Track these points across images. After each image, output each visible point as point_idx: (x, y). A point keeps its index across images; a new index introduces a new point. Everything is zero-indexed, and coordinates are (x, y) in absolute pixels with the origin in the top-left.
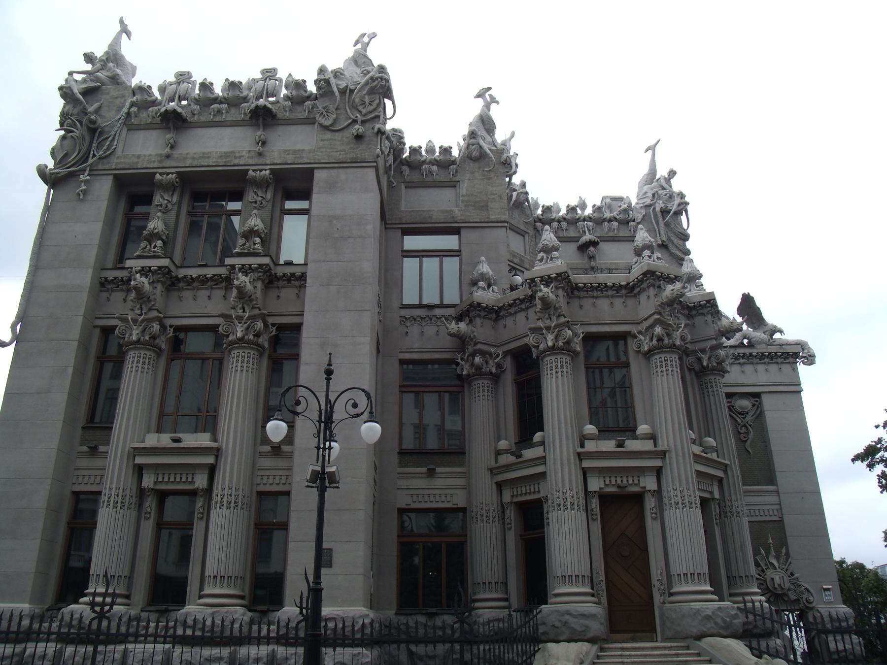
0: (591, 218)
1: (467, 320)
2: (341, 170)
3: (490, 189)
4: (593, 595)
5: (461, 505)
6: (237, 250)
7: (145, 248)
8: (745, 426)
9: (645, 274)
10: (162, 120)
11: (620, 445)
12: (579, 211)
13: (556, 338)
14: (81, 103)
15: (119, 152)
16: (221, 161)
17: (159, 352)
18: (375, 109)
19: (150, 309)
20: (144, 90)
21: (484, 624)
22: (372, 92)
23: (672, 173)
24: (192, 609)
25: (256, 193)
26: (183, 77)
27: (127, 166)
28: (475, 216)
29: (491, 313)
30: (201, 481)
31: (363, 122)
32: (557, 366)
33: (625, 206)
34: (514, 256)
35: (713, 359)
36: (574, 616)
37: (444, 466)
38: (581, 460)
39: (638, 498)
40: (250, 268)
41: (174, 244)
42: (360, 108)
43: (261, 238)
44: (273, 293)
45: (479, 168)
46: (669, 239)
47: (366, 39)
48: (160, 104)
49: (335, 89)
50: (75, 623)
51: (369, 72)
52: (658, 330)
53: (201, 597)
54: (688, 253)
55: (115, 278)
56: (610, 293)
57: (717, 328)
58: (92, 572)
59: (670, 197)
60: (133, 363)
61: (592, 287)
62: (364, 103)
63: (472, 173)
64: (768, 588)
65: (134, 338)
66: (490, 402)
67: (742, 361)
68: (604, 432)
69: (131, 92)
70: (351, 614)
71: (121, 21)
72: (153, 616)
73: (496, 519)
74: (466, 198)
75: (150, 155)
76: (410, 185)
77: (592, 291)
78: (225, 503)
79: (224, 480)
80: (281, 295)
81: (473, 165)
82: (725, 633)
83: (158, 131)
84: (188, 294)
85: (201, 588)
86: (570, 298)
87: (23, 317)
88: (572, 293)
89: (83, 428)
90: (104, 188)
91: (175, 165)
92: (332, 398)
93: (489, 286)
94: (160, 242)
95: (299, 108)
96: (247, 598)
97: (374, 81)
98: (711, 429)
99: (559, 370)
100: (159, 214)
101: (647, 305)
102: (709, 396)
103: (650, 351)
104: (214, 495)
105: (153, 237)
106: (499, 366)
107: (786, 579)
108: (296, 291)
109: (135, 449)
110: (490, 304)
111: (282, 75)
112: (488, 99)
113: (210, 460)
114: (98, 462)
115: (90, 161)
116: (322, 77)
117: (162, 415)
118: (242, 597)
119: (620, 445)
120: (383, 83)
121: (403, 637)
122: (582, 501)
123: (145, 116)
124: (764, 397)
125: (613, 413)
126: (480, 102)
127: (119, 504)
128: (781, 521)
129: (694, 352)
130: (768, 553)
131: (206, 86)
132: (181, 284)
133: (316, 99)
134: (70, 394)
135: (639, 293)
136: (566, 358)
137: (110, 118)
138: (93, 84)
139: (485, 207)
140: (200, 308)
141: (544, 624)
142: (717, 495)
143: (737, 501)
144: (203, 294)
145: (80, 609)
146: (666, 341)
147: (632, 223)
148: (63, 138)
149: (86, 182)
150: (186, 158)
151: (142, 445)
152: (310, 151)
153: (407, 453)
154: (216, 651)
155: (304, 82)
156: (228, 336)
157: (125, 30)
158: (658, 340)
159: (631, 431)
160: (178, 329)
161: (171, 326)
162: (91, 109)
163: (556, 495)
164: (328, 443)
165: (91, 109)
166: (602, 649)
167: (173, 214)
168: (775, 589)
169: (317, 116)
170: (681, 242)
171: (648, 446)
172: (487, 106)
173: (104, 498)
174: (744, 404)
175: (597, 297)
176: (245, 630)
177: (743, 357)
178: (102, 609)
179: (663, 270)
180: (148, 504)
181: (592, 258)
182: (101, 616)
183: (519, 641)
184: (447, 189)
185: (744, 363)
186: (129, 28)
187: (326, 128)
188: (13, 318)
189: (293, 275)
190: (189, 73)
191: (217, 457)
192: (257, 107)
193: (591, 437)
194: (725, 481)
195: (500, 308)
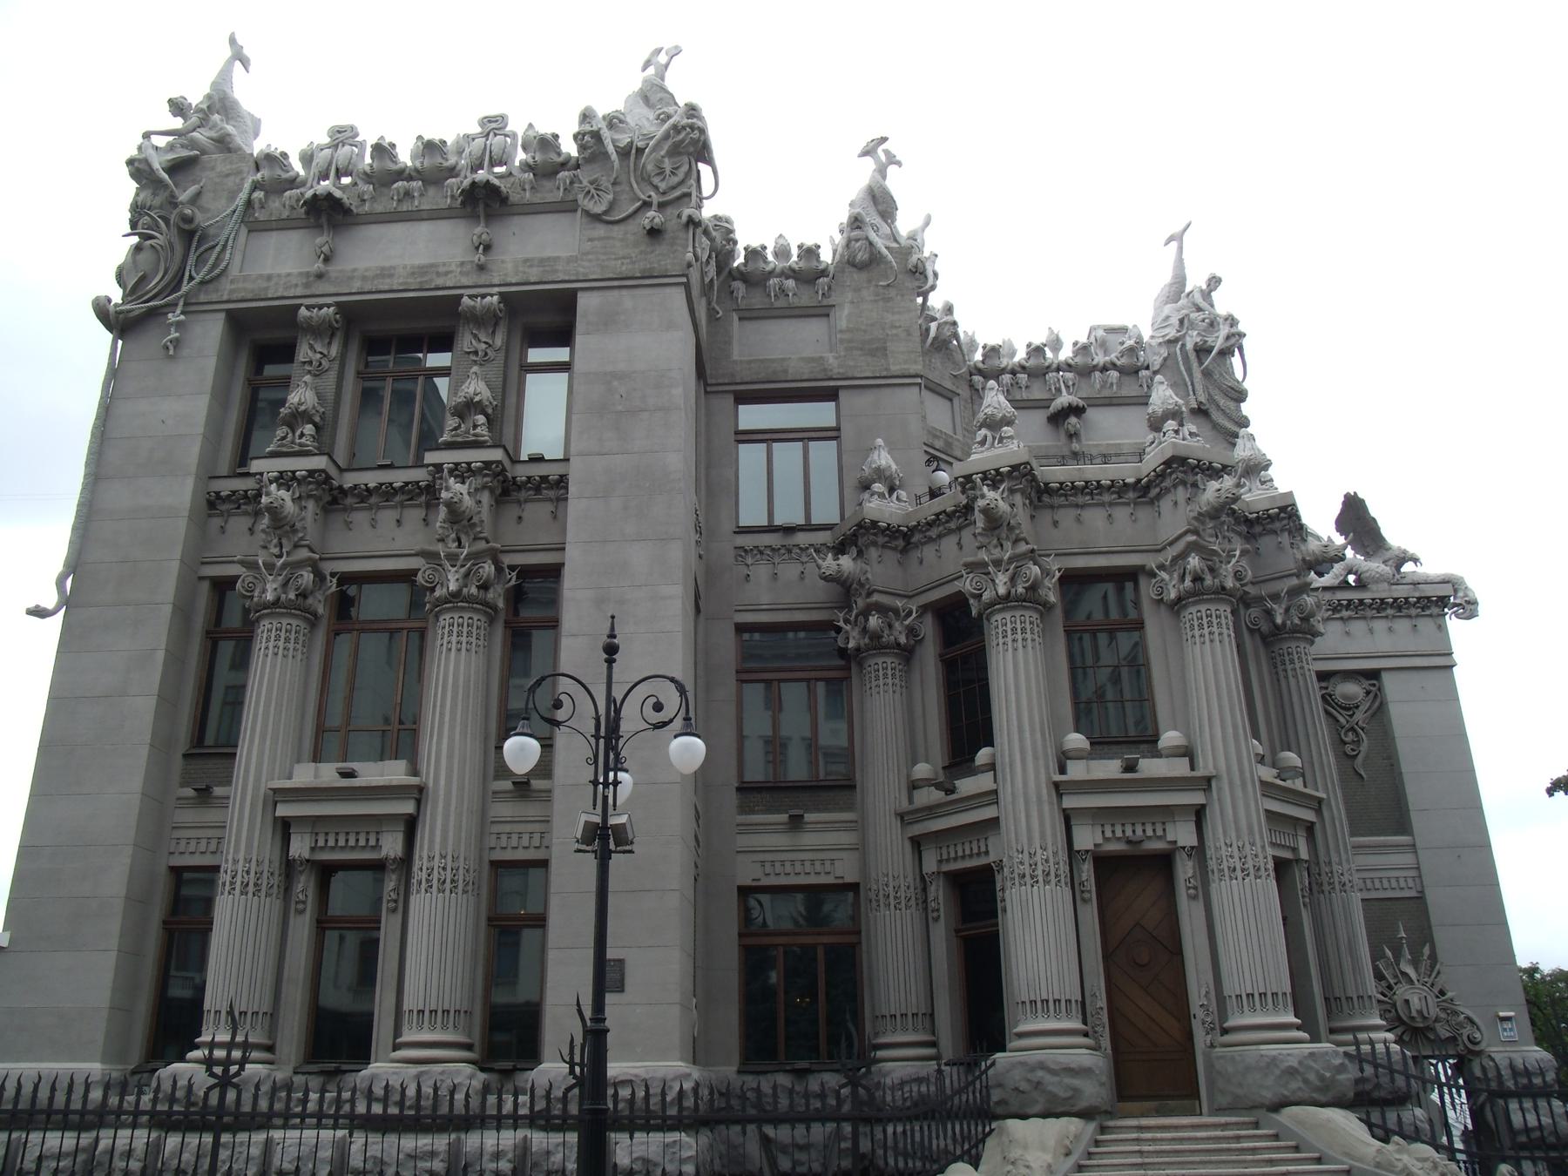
0: (1069, 365)
1: (854, 551)
2: (624, 292)
3: (889, 317)
4: (1086, 1035)
5: (849, 879)
6: (445, 437)
7: (283, 438)
8: (1352, 729)
9: (1168, 463)
10: (307, 213)
11: (1130, 767)
12: (1049, 354)
13: (1013, 579)
14: (166, 186)
15: (234, 271)
16: (413, 282)
17: (313, 620)
19: (296, 546)
20: (274, 160)
21: (893, 1088)
22: (675, 151)
23: (1214, 282)
24: (382, 1069)
25: (475, 336)
26: (343, 136)
27: (250, 296)
28: (863, 366)
30: (392, 845)
31: (662, 206)
32: (1014, 630)
33: (1132, 342)
34: (935, 436)
35: (1292, 611)
37: (819, 810)
38: (1060, 796)
39: (1164, 862)
40: (469, 469)
42: (656, 181)
43: (487, 415)
44: (511, 512)
45: (869, 281)
46: (1211, 399)
47: (663, 58)
48: (303, 184)
49: (611, 149)
50: (180, 1094)
51: (669, 117)
52: (1194, 562)
53: (396, 1047)
54: (1244, 423)
55: (234, 492)
56: (1106, 498)
57: (1299, 557)
58: (206, 1006)
59: (1212, 324)
60: (268, 640)
61: (1073, 487)
62: (661, 172)
63: (857, 290)
64: (1399, 1018)
65: (270, 596)
66: (897, 695)
67: (1345, 614)
68: (1101, 745)
69: (253, 165)
70: (660, 1074)
71: (232, 41)
72: (315, 1082)
73: (913, 902)
74: (846, 336)
75: (289, 275)
76: (748, 316)
77: (1075, 495)
78: (435, 882)
79: (431, 842)
80: (525, 515)
81: (859, 277)
82: (1323, 1099)
83: (302, 231)
84: (360, 518)
85: (397, 1032)
86: (1035, 508)
87: (75, 565)
88: (1039, 500)
89: (185, 756)
90: (210, 334)
91: (332, 290)
92: (618, 694)
93: (892, 490)
94: (310, 426)
95: (548, 184)
96: (477, 1047)
97: (679, 132)
98: (1292, 737)
99: (1019, 637)
100: (307, 378)
101: (1174, 517)
102: (1286, 677)
103: (1179, 599)
104: (415, 869)
105: (297, 418)
106: (911, 631)
107: (1432, 1001)
108: (549, 507)
109: (275, 791)
110: (894, 522)
111: (517, 126)
112: (883, 158)
113: (408, 808)
114: (211, 816)
115: (185, 288)
116: (587, 128)
117: (321, 730)
119: (1130, 767)
120: (696, 135)
121: (753, 1112)
122: (1064, 869)
123: (277, 207)
124: (1385, 677)
126: (869, 164)
127: (251, 888)
128: (1420, 899)
129: (1260, 600)
130: (1398, 955)
131: (383, 151)
132: (349, 501)
133: (578, 166)
134: (161, 697)
135: (1159, 497)
136: (1031, 616)
137: (218, 212)
138: (185, 153)
139: (878, 350)
140: (382, 541)
141: (1000, 1085)
142: (1304, 854)
143: (1340, 864)
144: (388, 516)
145: (188, 1071)
146: (1209, 581)
147: (1143, 373)
148: (137, 249)
149: (179, 325)
150: (351, 278)
151: (288, 784)
152: (570, 260)
153: (753, 789)
154: (424, 1142)
155: (556, 137)
156: (433, 590)
157: (239, 56)
158: (1194, 580)
159: (1148, 741)
160: (345, 579)
161: (333, 575)
162: (183, 197)
163: (1017, 857)
164: (611, 774)
165: (183, 197)
166: (1103, 1130)
167: (333, 375)
169: (580, 197)
170: (1232, 405)
171: (1180, 768)
172: (882, 171)
173: (224, 877)
174: (1351, 690)
175: (1083, 507)
176: (475, 1103)
177: (1347, 607)
178: (226, 1071)
179: (1200, 455)
180: (300, 887)
182: (225, 1082)
183: (957, 1116)
184: (814, 320)
185: (1350, 618)
186: (246, 51)
187: (596, 218)
188: (58, 566)
189: (544, 479)
190: (352, 128)
191: (419, 802)
192: (474, 184)
193: (1078, 755)
194: (1318, 827)
195: (912, 530)
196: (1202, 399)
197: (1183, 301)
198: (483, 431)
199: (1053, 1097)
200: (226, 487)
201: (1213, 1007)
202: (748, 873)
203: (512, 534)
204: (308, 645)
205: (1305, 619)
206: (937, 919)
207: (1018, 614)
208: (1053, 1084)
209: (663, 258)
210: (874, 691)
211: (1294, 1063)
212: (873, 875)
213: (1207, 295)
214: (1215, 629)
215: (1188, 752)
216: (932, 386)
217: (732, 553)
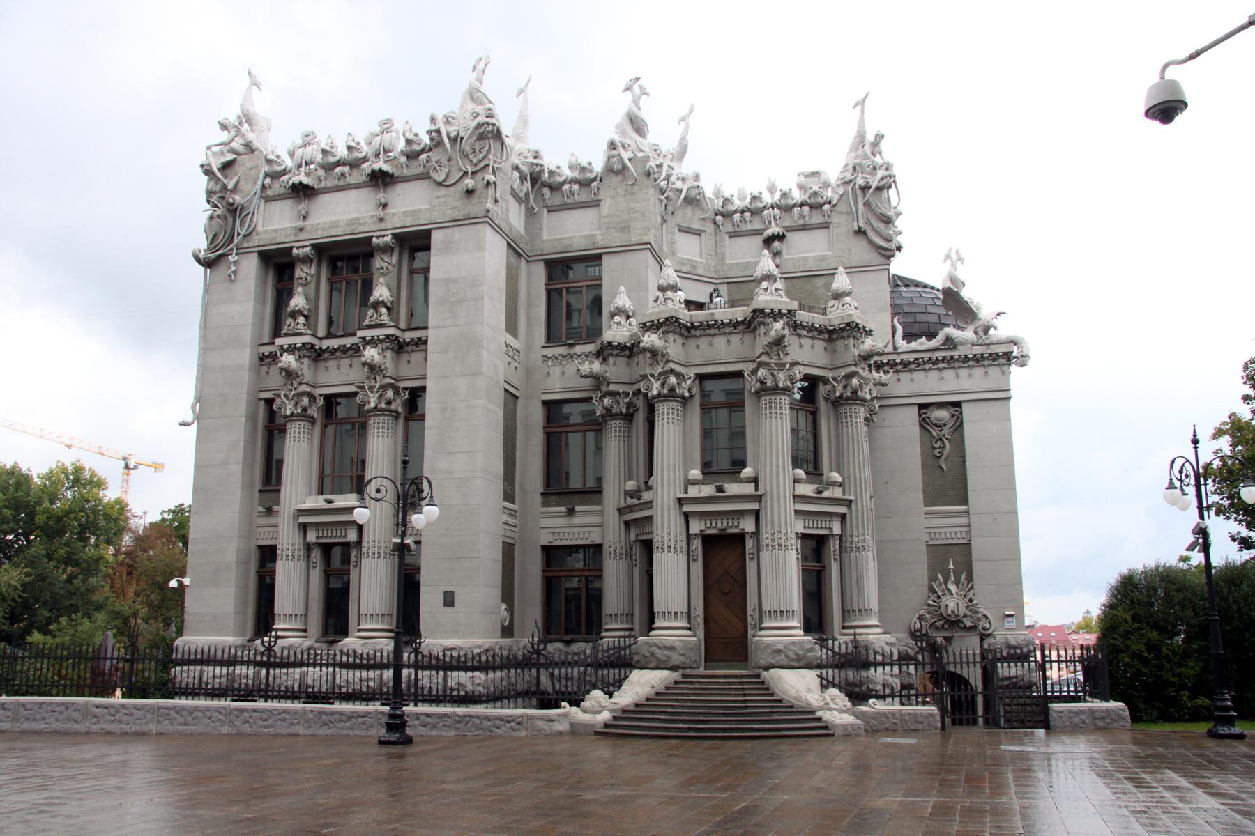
3: (633, 205)
5: (597, 542)
6: (367, 323)
11: (720, 489)
13: (663, 385)
15: (260, 228)
17: (313, 421)
18: (485, 157)
19: (300, 384)
22: (481, 137)
23: (879, 137)
24: (350, 643)
28: (616, 239)
41: (317, 315)
42: (471, 157)
44: (405, 357)
56: (727, 330)
57: (856, 353)
59: (875, 168)
63: (616, 188)
67: (941, 365)
71: (250, 74)
74: (607, 220)
76: (552, 209)
80: (412, 359)
81: (616, 180)
84: (332, 364)
87: (199, 399)
90: (250, 266)
93: (628, 317)
95: (415, 163)
100: (300, 289)
103: (757, 392)
106: (629, 405)
111: (399, 126)
114: (272, 520)
115: (236, 240)
117: (321, 477)
118: (390, 631)
119: (720, 489)
125: (724, 457)
128: (968, 545)
132: (326, 355)
135: (755, 329)
137: (247, 192)
138: (230, 157)
139: (626, 228)
140: (338, 377)
142: (837, 529)
144: (345, 362)
146: (769, 384)
148: (211, 218)
151: (303, 507)
157: (256, 84)
167: (313, 285)
170: (882, 226)
171: (749, 489)
172: (636, 102)
179: (773, 306)
186: (259, 79)
187: (440, 184)
188: (192, 400)
189: (419, 339)
192: (373, 171)
196: (861, 225)
197: (860, 151)
198: (385, 318)
199: (659, 660)
200: (267, 350)
201: (757, 615)
202: (546, 539)
203: (405, 371)
204: (311, 435)
205: (855, 392)
208: (661, 654)
209: (474, 208)
211: (780, 647)
213: (875, 144)
215: (755, 480)
217: (541, 359)
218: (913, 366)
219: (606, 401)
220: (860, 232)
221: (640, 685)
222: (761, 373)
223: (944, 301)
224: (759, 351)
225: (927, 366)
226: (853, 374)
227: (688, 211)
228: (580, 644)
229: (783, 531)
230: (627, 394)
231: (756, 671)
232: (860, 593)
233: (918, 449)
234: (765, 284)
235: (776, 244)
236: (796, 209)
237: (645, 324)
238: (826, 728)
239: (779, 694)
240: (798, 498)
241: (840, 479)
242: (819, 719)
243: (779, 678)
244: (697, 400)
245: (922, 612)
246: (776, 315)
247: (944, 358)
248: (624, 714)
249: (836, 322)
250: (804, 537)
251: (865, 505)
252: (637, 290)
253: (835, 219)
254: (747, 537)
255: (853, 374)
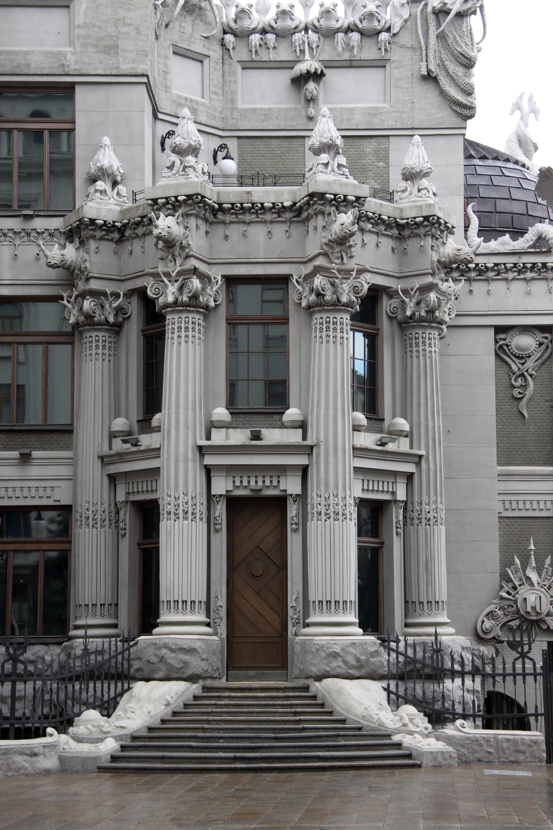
1: (77, 241)
3: (122, 13)
4: (208, 625)
5: (65, 502)
13: (181, 289)
29: (112, 232)
32: (180, 328)
35: (423, 305)
36: (172, 651)
37: (45, 449)
56: (268, 217)
57: (435, 258)
61: (242, 208)
67: (529, 275)
73: (107, 523)
77: (244, 213)
93: (115, 184)
99: (183, 334)
102: (411, 357)
103: (309, 307)
110: (110, 220)
119: (256, 436)
130: (525, 565)
135: (308, 219)
139: (112, 49)
141: (139, 658)
142: (401, 495)
143: (428, 504)
146: (328, 297)
168: (528, 613)
170: (460, 71)
171: (294, 437)
181: (311, 100)
183: (99, 678)
185: (533, 279)
194: (416, 477)
195: (125, 226)
196: (432, 67)
199: (171, 667)
205: (431, 312)
206: (124, 535)
207: (183, 316)
208: (173, 659)
210: (89, 358)
211: (337, 649)
212: (79, 502)
214: (331, 333)
215: (303, 426)
216: (181, 51)
218: (491, 274)
219: (88, 304)
220: (430, 78)
221: (147, 703)
222: (319, 281)
223: (539, 186)
224: (313, 249)
225: (511, 275)
226: (431, 287)
227: (188, 24)
228: (37, 648)
229: (341, 495)
230: (117, 296)
231: (301, 682)
232: (430, 581)
233: (494, 387)
234: (324, 157)
235: (311, 85)
236: (341, 35)
237: (155, 201)
238: (409, 756)
239: (341, 711)
240: (359, 452)
241: (407, 428)
242: (398, 745)
243: (340, 691)
244: (223, 310)
245: (491, 608)
246: (341, 203)
247: (534, 264)
248: (134, 743)
249: (410, 214)
250: (362, 503)
251: (437, 461)
252: (125, 144)
253: (396, 55)
254: (290, 501)
255: (431, 287)
